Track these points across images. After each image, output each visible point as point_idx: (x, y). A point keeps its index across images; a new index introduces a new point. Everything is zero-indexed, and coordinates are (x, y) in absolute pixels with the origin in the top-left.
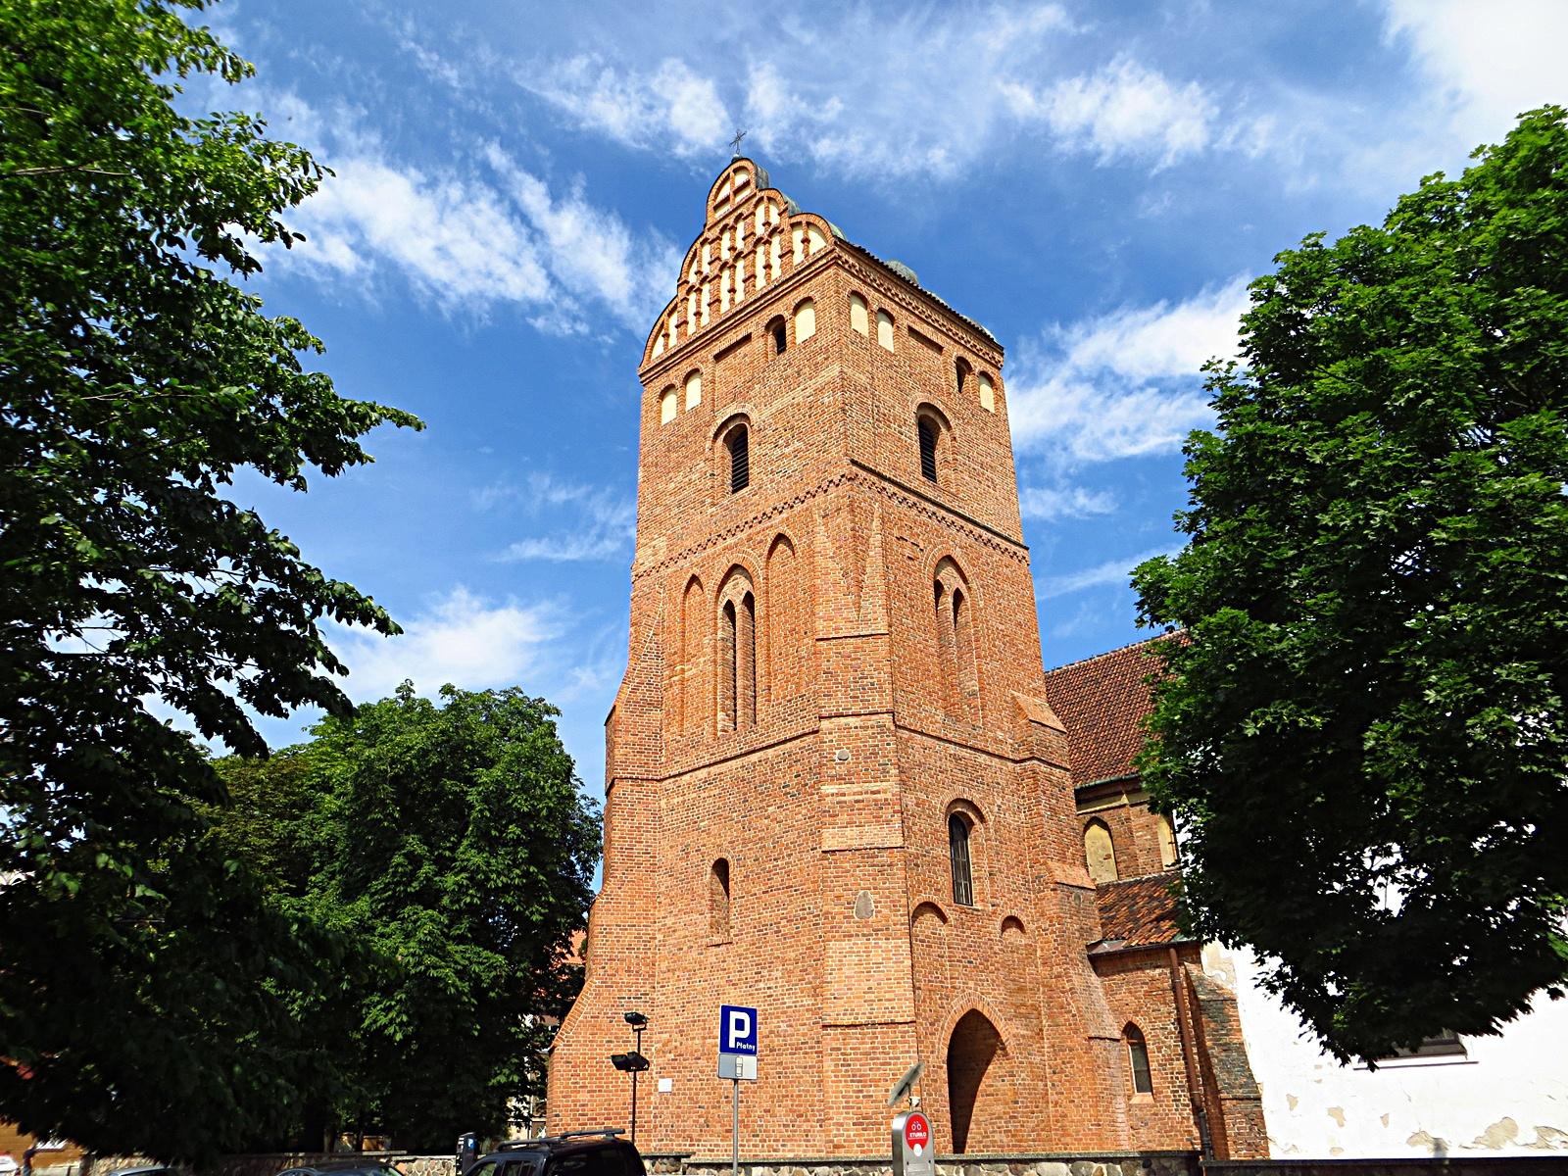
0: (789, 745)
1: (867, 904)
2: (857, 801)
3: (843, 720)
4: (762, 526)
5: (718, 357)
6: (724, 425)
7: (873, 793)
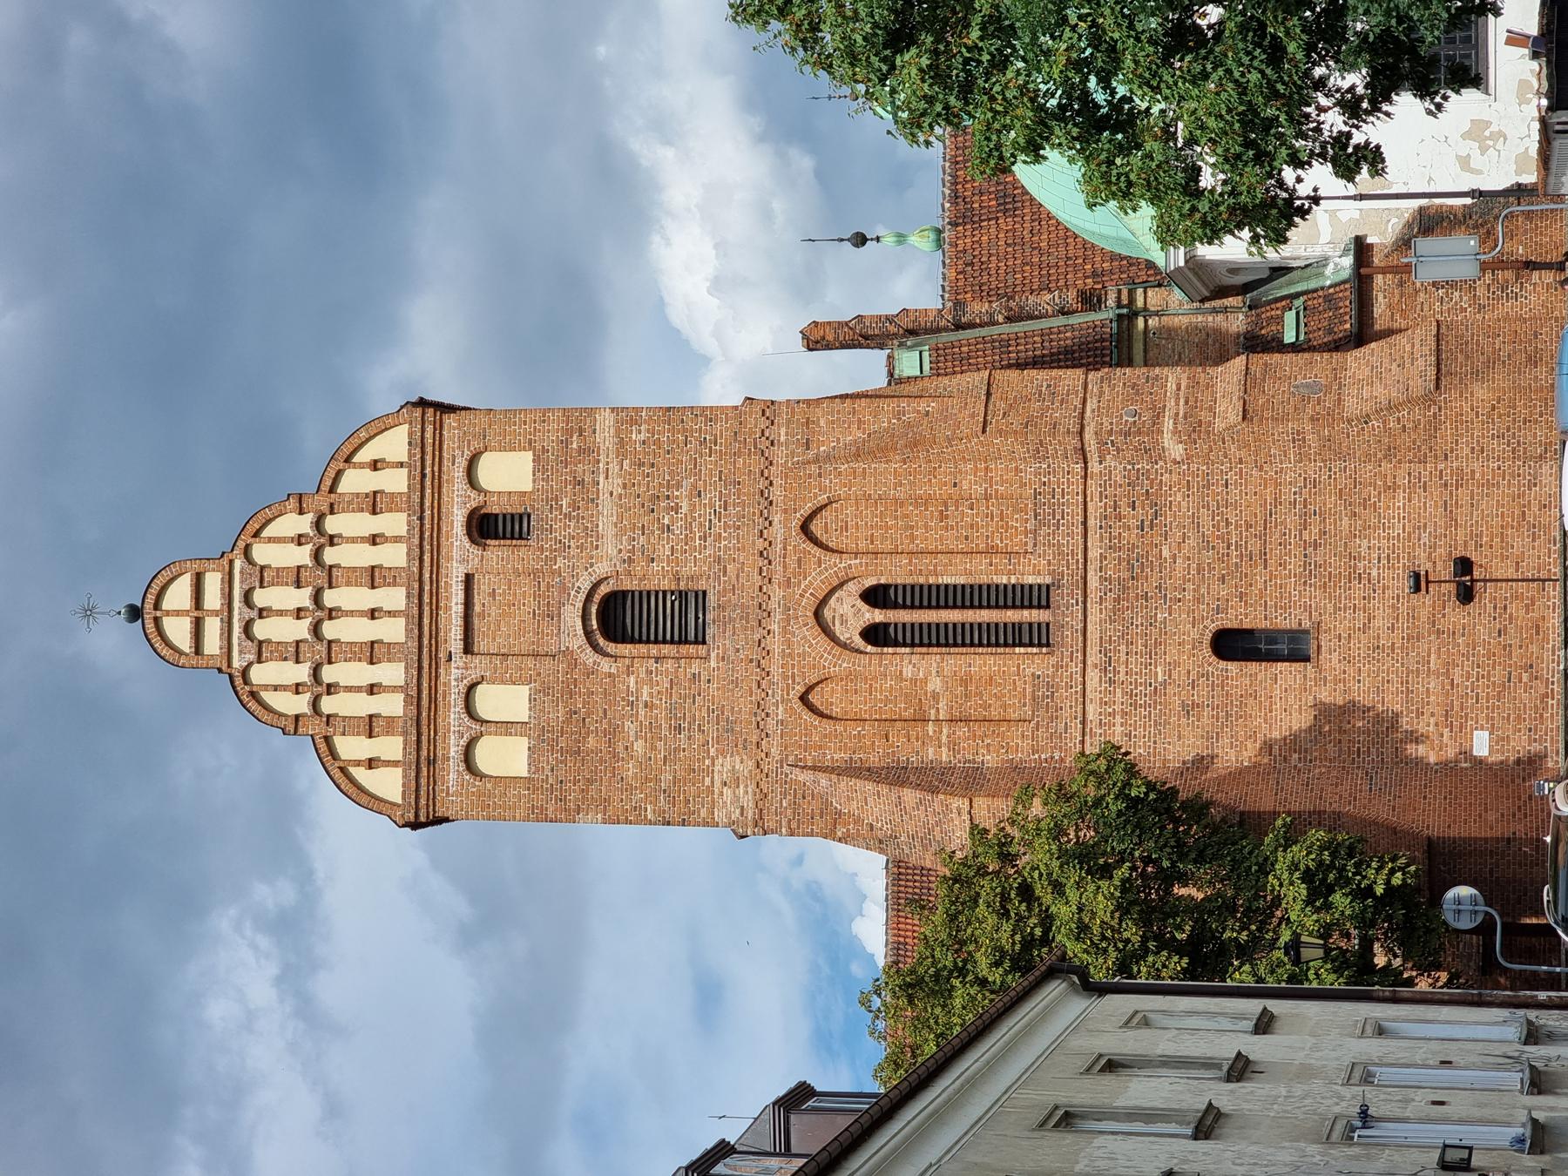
0: (1091, 522)
1: (1307, 386)
2: (1186, 403)
3: (1088, 413)
4: (777, 561)
5: (468, 649)
6: (588, 634)
7: (1179, 389)
